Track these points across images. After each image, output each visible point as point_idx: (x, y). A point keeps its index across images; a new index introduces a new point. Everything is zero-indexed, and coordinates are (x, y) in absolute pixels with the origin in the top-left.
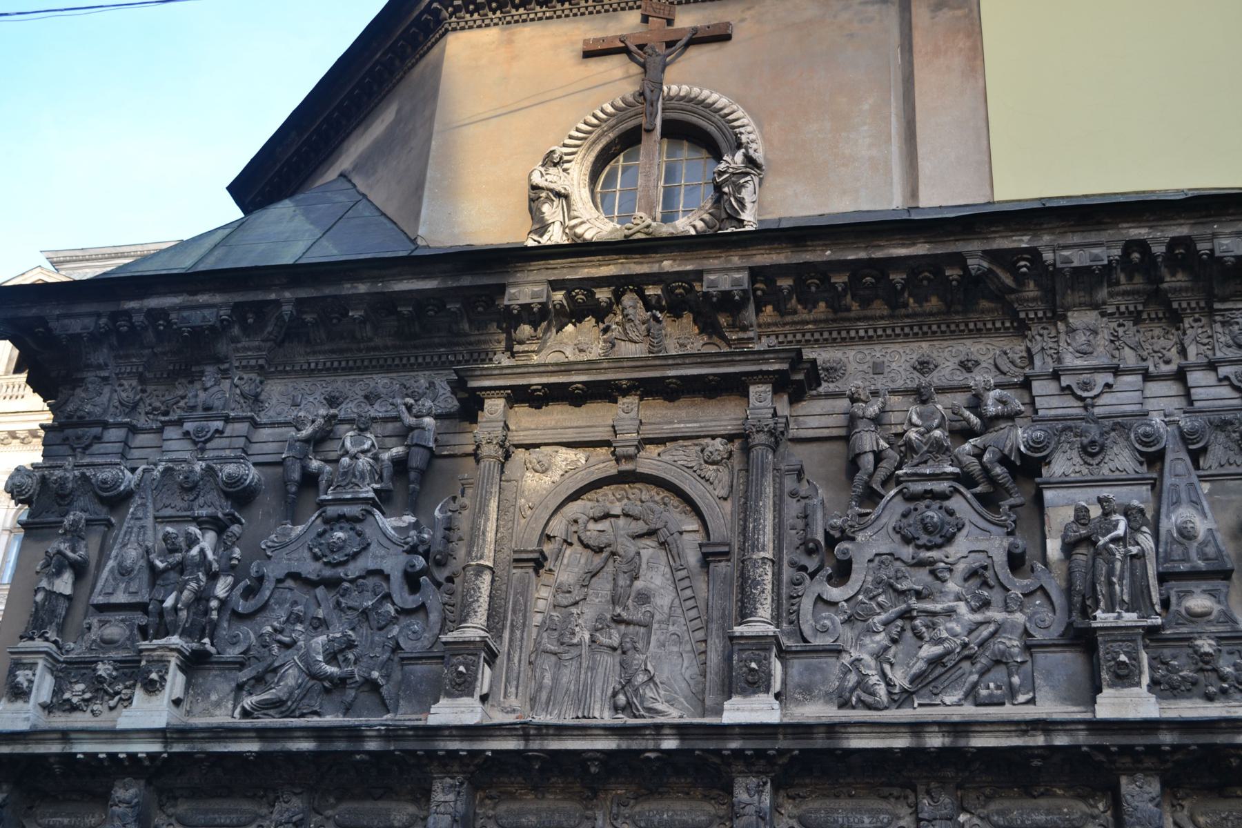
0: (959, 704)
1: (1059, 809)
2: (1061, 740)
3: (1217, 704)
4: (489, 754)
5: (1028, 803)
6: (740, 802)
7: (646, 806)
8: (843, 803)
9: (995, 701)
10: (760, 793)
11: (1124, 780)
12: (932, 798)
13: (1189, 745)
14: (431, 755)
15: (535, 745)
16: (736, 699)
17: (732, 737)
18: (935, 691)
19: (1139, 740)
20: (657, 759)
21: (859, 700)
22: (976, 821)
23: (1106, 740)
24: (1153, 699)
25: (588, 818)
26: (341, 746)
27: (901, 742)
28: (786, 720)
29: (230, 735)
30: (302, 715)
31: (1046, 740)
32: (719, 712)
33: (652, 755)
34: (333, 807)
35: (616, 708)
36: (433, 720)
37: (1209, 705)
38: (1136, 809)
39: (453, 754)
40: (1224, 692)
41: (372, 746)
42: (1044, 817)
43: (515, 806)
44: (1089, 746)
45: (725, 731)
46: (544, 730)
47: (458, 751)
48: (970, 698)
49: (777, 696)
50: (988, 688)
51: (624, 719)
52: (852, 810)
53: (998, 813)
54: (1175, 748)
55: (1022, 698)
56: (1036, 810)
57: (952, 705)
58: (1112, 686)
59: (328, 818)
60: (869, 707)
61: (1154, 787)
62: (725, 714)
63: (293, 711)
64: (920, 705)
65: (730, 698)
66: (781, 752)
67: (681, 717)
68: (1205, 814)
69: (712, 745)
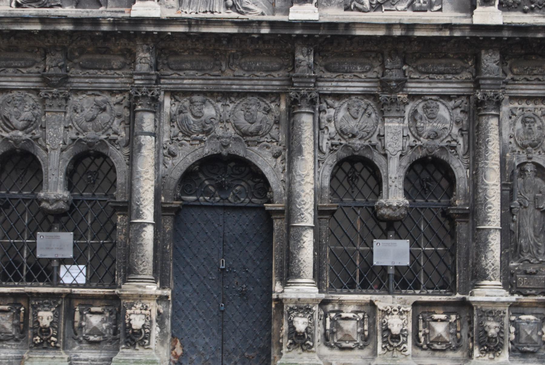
0: (404, 10)
1: (451, 64)
2: (457, 34)
3: (528, 15)
4: (170, 34)
5: (436, 61)
6: (299, 60)
7: (248, 60)
8: (347, 60)
9: (423, 9)
10: (308, 55)
11: (483, 52)
12: (392, 58)
13: (516, 38)
14: (137, 34)
15: (194, 30)
16: (295, 7)
17: (298, 28)
18: (393, 3)
19: (493, 35)
20: (258, 38)
21: (355, 7)
22: (411, 69)
23: (478, 35)
24: (500, 12)
25: (217, 65)
26: (88, 28)
27: (381, 33)
28: (323, 20)
29: (24, 21)
30: (51, 7)
31: (450, 34)
32: (287, 12)
33: (256, 36)
34: (77, 57)
35: (227, 7)
36: (134, 14)
37: (525, 15)
38: (488, 66)
39: (149, 34)
40: (532, 10)
41: (105, 28)
42: (443, 68)
43: (178, 59)
44: (471, 37)
45: (292, 24)
46: (199, 22)
47: (152, 32)
48: (410, 7)
49: (317, 5)
50: (420, 2)
51: (234, 15)
52: (352, 63)
53: (424, 66)
54: (509, 38)
55: (436, 8)
56: (440, 64)
57: (401, 11)
58: (481, 5)
59: (75, 64)
60: (360, 10)
61: (497, 57)
62: (290, 14)
63: (46, 4)
64: (385, 10)
65: (292, 6)
66: (321, 36)
67: (263, 14)
68: (517, 67)
69: (286, 32)
